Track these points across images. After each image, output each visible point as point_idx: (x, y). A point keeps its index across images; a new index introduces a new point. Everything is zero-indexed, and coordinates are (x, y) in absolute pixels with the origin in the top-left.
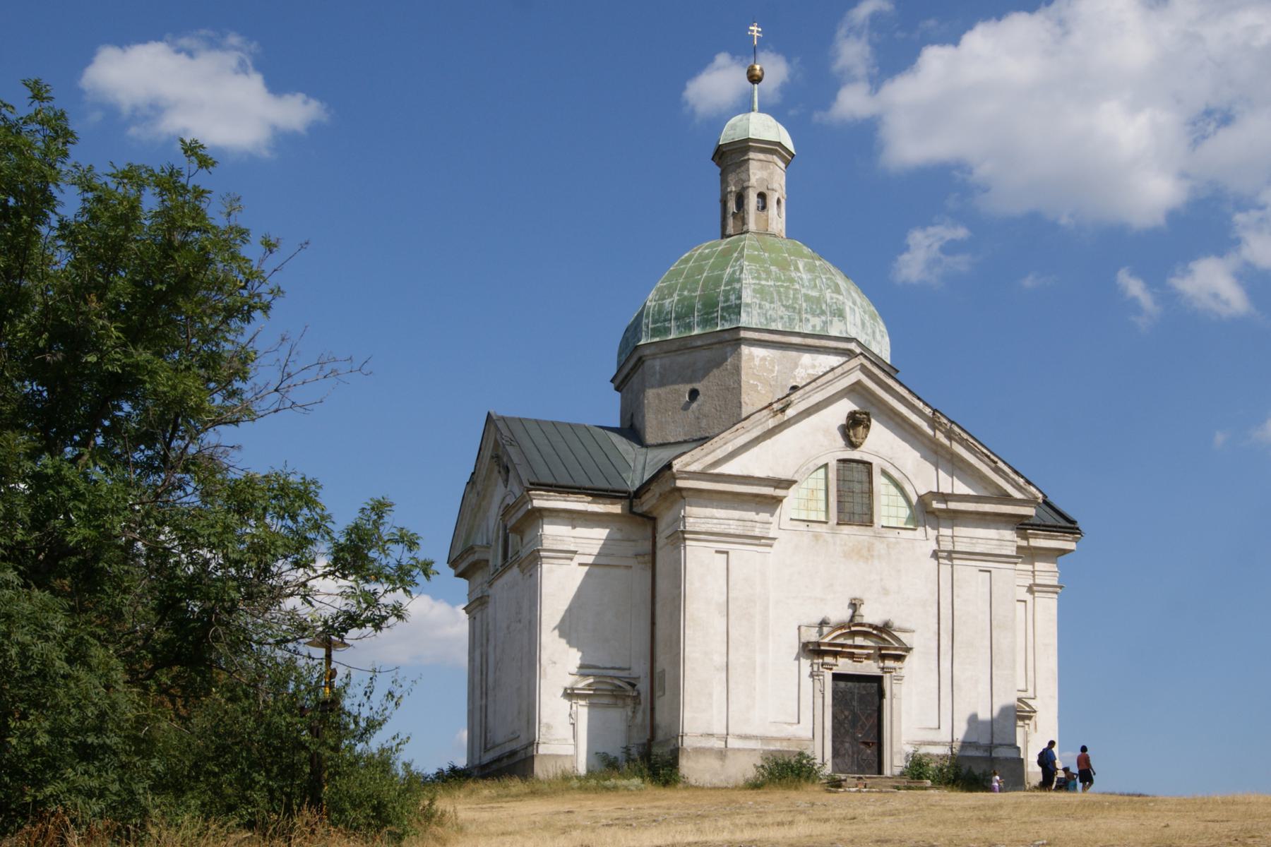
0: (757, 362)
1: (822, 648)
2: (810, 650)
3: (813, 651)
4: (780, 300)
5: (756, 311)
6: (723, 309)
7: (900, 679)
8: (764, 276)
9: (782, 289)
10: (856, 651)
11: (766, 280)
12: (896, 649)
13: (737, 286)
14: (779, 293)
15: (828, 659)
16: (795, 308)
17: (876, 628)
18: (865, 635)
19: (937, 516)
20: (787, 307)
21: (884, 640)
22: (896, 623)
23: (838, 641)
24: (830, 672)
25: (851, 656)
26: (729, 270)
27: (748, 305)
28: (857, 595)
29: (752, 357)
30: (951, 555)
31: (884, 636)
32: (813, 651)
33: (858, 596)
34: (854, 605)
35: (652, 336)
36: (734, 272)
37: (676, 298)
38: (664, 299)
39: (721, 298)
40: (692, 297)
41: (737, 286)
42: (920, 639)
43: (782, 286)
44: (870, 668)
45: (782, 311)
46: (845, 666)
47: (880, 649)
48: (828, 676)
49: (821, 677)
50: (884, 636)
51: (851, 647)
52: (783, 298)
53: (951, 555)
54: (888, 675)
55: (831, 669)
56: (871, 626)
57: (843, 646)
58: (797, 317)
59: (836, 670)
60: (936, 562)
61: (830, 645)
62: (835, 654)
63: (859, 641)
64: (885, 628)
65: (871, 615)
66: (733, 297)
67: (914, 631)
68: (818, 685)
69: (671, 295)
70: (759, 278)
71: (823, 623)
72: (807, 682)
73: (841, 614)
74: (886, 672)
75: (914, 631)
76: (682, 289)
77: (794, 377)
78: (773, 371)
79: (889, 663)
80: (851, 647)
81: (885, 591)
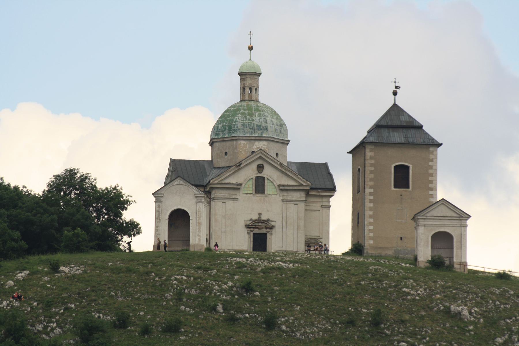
0: (242, 145)
1: (250, 226)
3: (248, 226)
4: (249, 127)
5: (242, 131)
6: (233, 130)
8: (245, 119)
9: (250, 124)
11: (246, 121)
12: (270, 226)
13: (237, 123)
14: (249, 125)
15: (252, 229)
16: (253, 129)
17: (264, 221)
18: (262, 222)
20: (251, 129)
21: (266, 224)
23: (254, 225)
25: (258, 228)
26: (236, 118)
27: (239, 129)
28: (260, 212)
29: (241, 144)
30: (287, 201)
32: (248, 226)
34: (260, 214)
35: (216, 136)
36: (237, 119)
37: (222, 125)
38: (219, 125)
39: (233, 127)
40: (226, 125)
41: (237, 123)
43: (250, 122)
44: (264, 231)
45: (249, 130)
46: (256, 231)
47: (265, 226)
48: (252, 234)
51: (257, 226)
52: (250, 126)
53: (287, 201)
56: (263, 220)
57: (255, 226)
58: (254, 131)
59: (254, 232)
61: (251, 225)
62: (254, 228)
63: (260, 224)
64: (268, 220)
65: (264, 217)
66: (235, 127)
68: (249, 236)
69: (221, 123)
70: (243, 120)
71: (251, 220)
72: (247, 236)
73: (255, 217)
76: (224, 122)
77: (253, 149)
78: (247, 147)
81: (268, 211)
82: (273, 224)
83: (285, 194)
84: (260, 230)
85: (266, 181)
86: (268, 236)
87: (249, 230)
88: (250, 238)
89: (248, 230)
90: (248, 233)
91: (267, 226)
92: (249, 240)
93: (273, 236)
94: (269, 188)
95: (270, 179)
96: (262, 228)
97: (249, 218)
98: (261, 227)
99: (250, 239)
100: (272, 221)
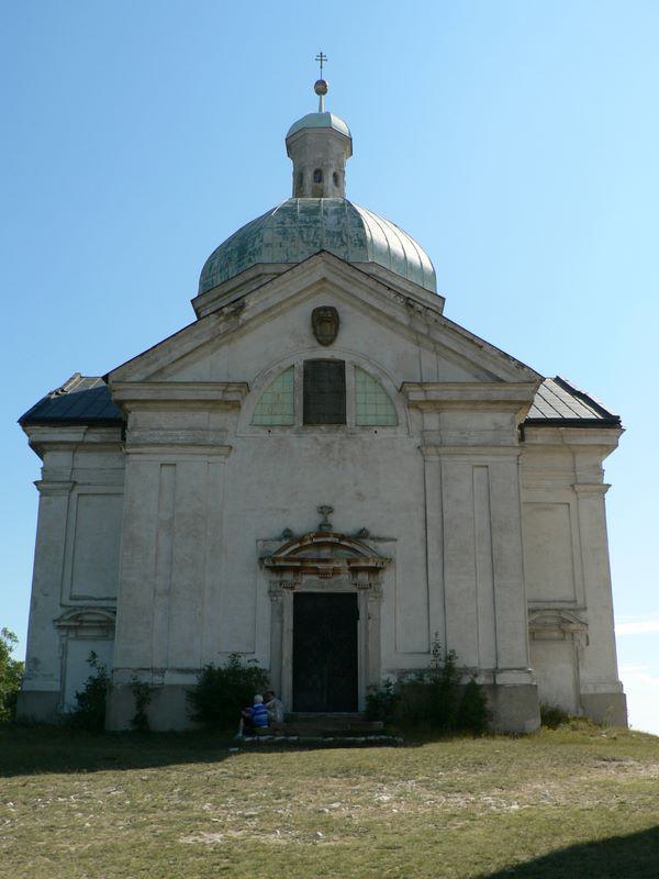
2: (267, 567)
3: (273, 565)
7: (379, 596)
10: (319, 566)
15: (288, 577)
17: (343, 537)
19: (421, 410)
22: (374, 532)
24: (291, 592)
25: (316, 571)
28: (327, 502)
31: (353, 545)
33: (328, 504)
34: (325, 510)
42: (404, 548)
44: (343, 583)
46: (309, 584)
48: (288, 597)
49: (280, 598)
50: (353, 545)
51: (313, 561)
54: (362, 592)
55: (292, 588)
56: (336, 535)
57: (302, 560)
59: (298, 589)
60: (420, 458)
61: (286, 559)
62: (296, 570)
63: (325, 553)
64: (362, 534)
65: (344, 523)
67: (396, 540)
73: (304, 522)
74: (360, 589)
75: (396, 540)
79: (363, 578)
80: (313, 561)
81: (360, 496)
82: (383, 548)
83: (431, 421)
84: (326, 582)
85: (350, 377)
86: (364, 605)
87: (275, 578)
88: (281, 613)
89: (270, 582)
90: (271, 593)
91: (357, 561)
92: (278, 625)
93: (385, 607)
94: (361, 399)
95: (368, 368)
96: (336, 572)
97: (278, 530)
98: (331, 566)
99: (282, 622)
100: (379, 539)
